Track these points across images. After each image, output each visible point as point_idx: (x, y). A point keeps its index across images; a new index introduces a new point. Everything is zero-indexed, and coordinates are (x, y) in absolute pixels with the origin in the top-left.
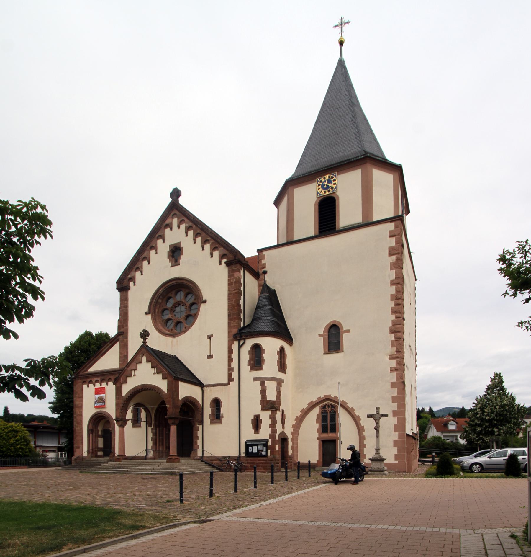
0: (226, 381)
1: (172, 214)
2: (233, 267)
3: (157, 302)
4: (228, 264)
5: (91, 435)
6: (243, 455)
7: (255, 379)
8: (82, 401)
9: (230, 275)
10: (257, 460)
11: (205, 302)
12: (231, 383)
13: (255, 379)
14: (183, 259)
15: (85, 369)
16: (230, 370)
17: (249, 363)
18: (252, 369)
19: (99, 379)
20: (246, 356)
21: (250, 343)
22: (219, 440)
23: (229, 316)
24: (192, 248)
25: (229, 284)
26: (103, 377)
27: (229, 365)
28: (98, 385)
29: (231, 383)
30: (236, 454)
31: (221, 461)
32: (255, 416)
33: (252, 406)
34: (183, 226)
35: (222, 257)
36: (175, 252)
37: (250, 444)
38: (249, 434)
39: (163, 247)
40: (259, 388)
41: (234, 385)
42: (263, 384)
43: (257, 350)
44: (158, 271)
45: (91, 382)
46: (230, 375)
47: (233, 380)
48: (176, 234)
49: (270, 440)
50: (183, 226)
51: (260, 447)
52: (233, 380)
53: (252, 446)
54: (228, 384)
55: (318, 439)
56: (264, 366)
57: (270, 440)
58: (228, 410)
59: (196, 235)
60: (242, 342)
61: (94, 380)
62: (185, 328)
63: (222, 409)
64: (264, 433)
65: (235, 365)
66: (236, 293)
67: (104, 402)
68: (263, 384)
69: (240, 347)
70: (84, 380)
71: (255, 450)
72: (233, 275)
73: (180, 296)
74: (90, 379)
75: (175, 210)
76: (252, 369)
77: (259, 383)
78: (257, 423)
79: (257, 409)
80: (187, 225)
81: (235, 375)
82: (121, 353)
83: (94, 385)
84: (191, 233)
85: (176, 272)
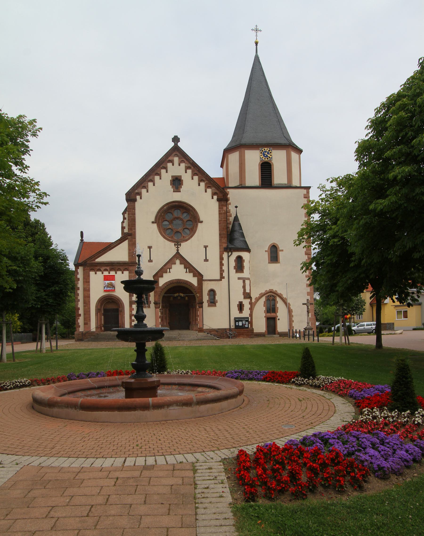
1: (174, 154)
2: (223, 203)
3: (161, 215)
4: (218, 200)
5: (99, 313)
6: (233, 326)
7: (239, 278)
8: (89, 285)
9: (220, 208)
10: (242, 331)
11: (202, 222)
12: (223, 280)
13: (239, 278)
14: (184, 188)
15: (93, 259)
16: (222, 271)
17: (235, 268)
18: (237, 272)
19: (108, 268)
20: (233, 264)
21: (235, 254)
22: (215, 317)
23: (220, 235)
24: (190, 182)
25: (220, 214)
26: (112, 267)
27: (221, 268)
28: (106, 273)
29: (223, 280)
30: (227, 327)
31: (217, 331)
32: (239, 302)
33: (237, 296)
34: (183, 165)
35: (214, 194)
36: (177, 182)
37: (237, 320)
38: (235, 313)
39: (166, 177)
40: (242, 284)
41: (225, 281)
42: (244, 282)
43: (239, 260)
45: (99, 270)
46: (221, 274)
47: (224, 278)
48: (177, 169)
49: (250, 318)
50: (183, 165)
51: (244, 322)
52: (224, 278)
53: (238, 321)
54: (221, 280)
55: (265, 317)
56: (245, 270)
57: (250, 318)
59: (194, 174)
60: (230, 254)
61: (102, 269)
62: (183, 237)
63: (216, 297)
64: (246, 313)
65: (225, 268)
66: (224, 220)
67: (114, 287)
68: (244, 282)
69: (229, 257)
70: (92, 268)
71: (240, 324)
72: (222, 208)
73: (185, 217)
74: (98, 268)
75: (176, 151)
76: (237, 272)
77: (241, 281)
78: (241, 307)
79: (241, 298)
80: (186, 165)
81: (225, 274)
82: (129, 250)
83: (103, 273)
84: (189, 171)
85: (177, 197)
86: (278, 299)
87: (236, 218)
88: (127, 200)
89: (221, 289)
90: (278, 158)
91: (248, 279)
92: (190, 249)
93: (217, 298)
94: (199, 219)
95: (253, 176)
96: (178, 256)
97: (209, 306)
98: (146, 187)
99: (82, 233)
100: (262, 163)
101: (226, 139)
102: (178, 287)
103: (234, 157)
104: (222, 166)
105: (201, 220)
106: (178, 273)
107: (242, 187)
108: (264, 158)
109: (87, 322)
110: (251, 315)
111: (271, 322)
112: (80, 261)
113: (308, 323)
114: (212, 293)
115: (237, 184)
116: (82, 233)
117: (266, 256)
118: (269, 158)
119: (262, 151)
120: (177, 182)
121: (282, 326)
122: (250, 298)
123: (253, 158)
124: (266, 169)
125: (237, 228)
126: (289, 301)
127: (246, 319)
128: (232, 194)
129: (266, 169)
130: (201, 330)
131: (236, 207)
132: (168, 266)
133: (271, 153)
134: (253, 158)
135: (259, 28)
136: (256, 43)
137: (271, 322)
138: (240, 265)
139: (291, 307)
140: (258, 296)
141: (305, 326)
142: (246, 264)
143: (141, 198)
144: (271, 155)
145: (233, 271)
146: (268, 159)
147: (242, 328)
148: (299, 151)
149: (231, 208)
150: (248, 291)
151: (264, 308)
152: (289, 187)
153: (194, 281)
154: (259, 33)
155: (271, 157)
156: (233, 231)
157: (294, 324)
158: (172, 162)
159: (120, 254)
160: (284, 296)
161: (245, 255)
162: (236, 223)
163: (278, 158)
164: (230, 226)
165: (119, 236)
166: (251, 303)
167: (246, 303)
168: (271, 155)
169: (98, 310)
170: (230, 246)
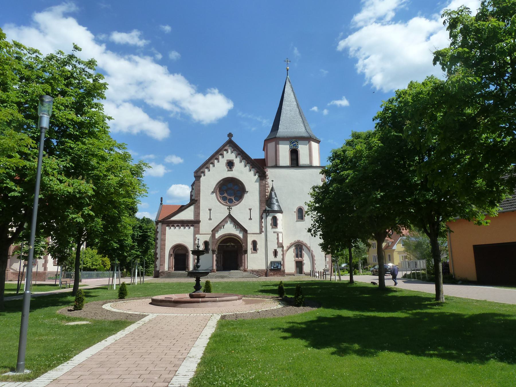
0: (258, 232)
7: (274, 232)
13: (274, 232)
14: (234, 169)
16: (261, 227)
17: (271, 225)
21: (272, 215)
36: (230, 164)
41: (263, 234)
42: (278, 235)
43: (275, 220)
44: (218, 173)
47: (263, 232)
48: (230, 155)
52: (263, 232)
58: (260, 246)
60: (268, 214)
61: (175, 225)
64: (279, 258)
77: (276, 234)
78: (275, 253)
79: (276, 247)
81: (263, 229)
85: (230, 174)
86: (304, 247)
87: (272, 189)
88: (195, 177)
89: (260, 240)
91: (281, 233)
92: (239, 211)
93: (258, 246)
94: (245, 190)
96: (230, 217)
97: (252, 253)
98: (208, 168)
99: (162, 198)
102: (229, 239)
103: (271, 146)
104: (264, 150)
105: (247, 190)
106: (229, 229)
107: (276, 166)
109: (162, 264)
110: (283, 259)
111: (299, 265)
112: (160, 219)
113: (326, 266)
114: (254, 243)
115: (274, 164)
116: (162, 198)
117: (295, 216)
120: (230, 164)
121: (307, 268)
122: (283, 247)
124: (294, 154)
125: (274, 196)
126: (311, 249)
127: (279, 263)
128: (270, 172)
130: (245, 271)
131: (272, 181)
132: (222, 224)
137: (299, 265)
138: (275, 223)
139: (314, 253)
140: (289, 245)
141: (324, 267)
142: (279, 222)
143: (205, 175)
145: (269, 227)
147: (276, 268)
149: (269, 181)
150: (281, 241)
151: (294, 254)
152: (311, 167)
153: (241, 235)
156: (270, 198)
157: (316, 266)
158: (226, 150)
159: (188, 215)
160: (309, 245)
161: (279, 216)
162: (273, 193)
164: (268, 194)
165: (188, 202)
166: (283, 251)
167: (279, 251)
169: (170, 255)
170: (268, 209)
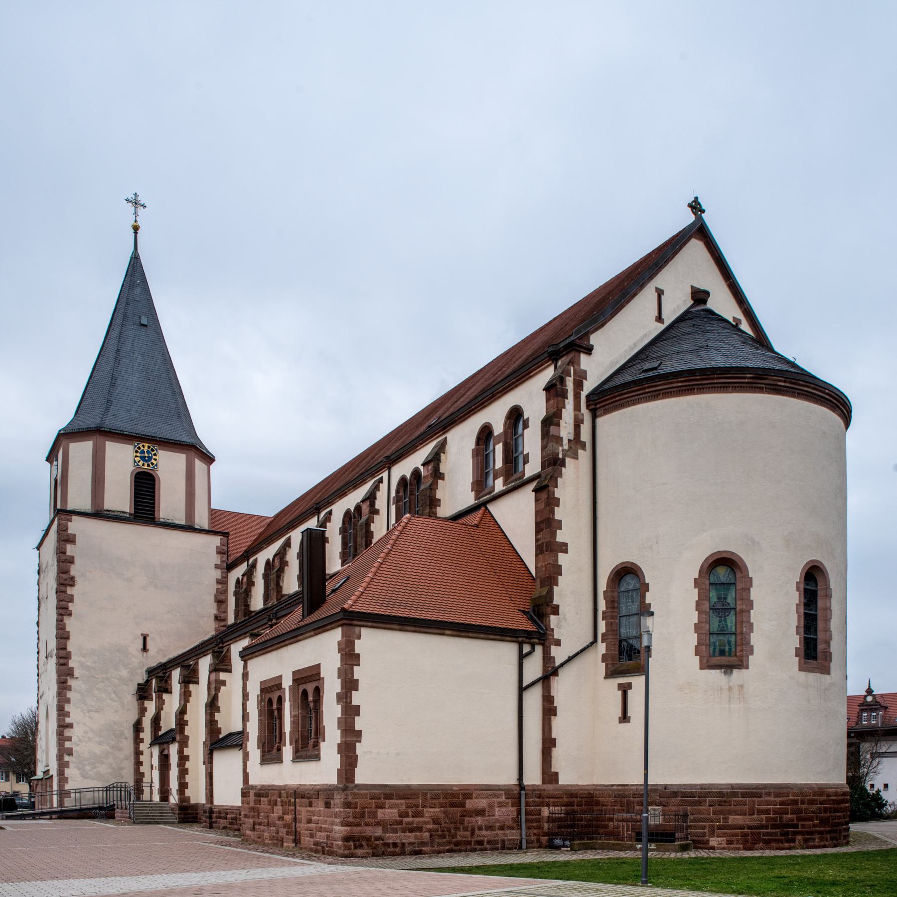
90: (170, 467)
95: (119, 496)
100: (138, 474)
101: (64, 417)
108: (141, 462)
118: (152, 464)
119: (139, 448)
123: (121, 460)
124: (145, 485)
129: (145, 485)
133: (155, 455)
134: (121, 460)
135: (142, 199)
136: (136, 229)
144: (155, 460)
146: (148, 465)
148: (209, 459)
154: (140, 210)
155: (155, 463)
163: (170, 467)
168: (155, 460)
